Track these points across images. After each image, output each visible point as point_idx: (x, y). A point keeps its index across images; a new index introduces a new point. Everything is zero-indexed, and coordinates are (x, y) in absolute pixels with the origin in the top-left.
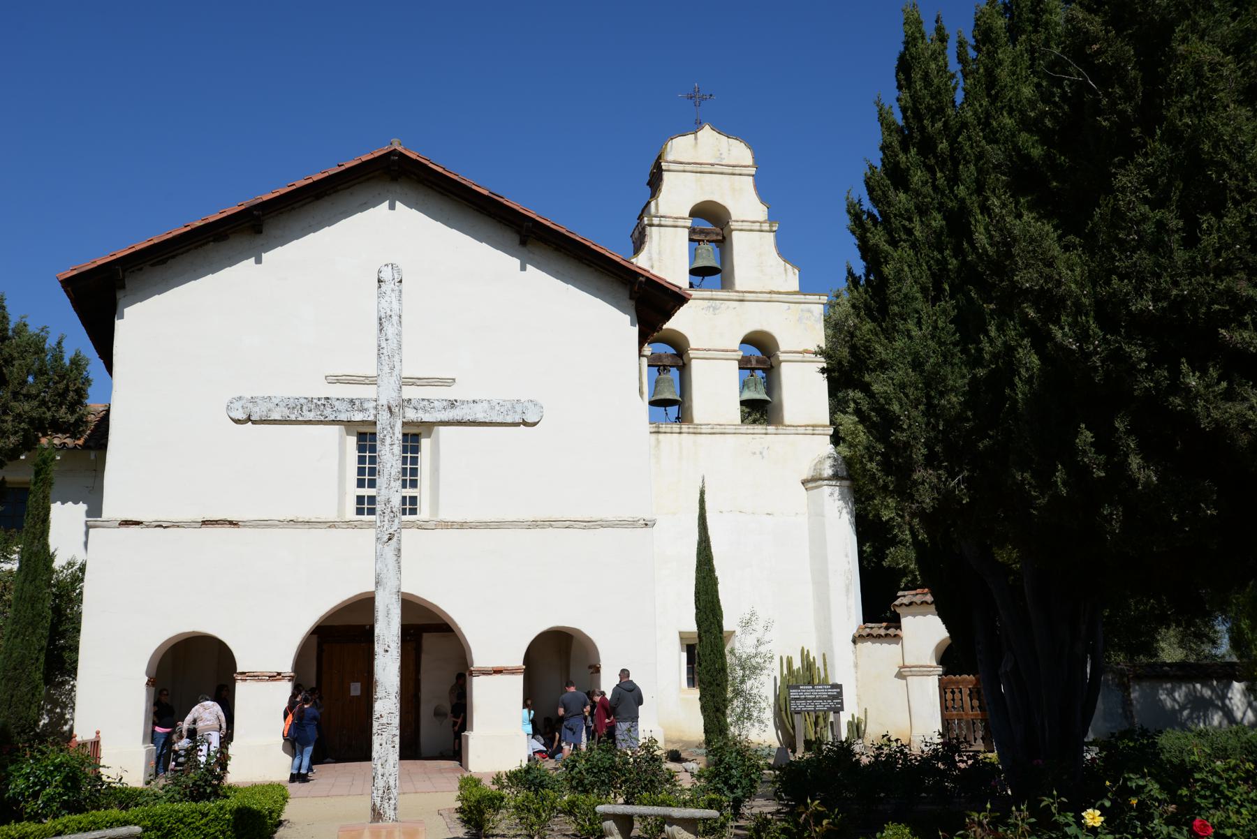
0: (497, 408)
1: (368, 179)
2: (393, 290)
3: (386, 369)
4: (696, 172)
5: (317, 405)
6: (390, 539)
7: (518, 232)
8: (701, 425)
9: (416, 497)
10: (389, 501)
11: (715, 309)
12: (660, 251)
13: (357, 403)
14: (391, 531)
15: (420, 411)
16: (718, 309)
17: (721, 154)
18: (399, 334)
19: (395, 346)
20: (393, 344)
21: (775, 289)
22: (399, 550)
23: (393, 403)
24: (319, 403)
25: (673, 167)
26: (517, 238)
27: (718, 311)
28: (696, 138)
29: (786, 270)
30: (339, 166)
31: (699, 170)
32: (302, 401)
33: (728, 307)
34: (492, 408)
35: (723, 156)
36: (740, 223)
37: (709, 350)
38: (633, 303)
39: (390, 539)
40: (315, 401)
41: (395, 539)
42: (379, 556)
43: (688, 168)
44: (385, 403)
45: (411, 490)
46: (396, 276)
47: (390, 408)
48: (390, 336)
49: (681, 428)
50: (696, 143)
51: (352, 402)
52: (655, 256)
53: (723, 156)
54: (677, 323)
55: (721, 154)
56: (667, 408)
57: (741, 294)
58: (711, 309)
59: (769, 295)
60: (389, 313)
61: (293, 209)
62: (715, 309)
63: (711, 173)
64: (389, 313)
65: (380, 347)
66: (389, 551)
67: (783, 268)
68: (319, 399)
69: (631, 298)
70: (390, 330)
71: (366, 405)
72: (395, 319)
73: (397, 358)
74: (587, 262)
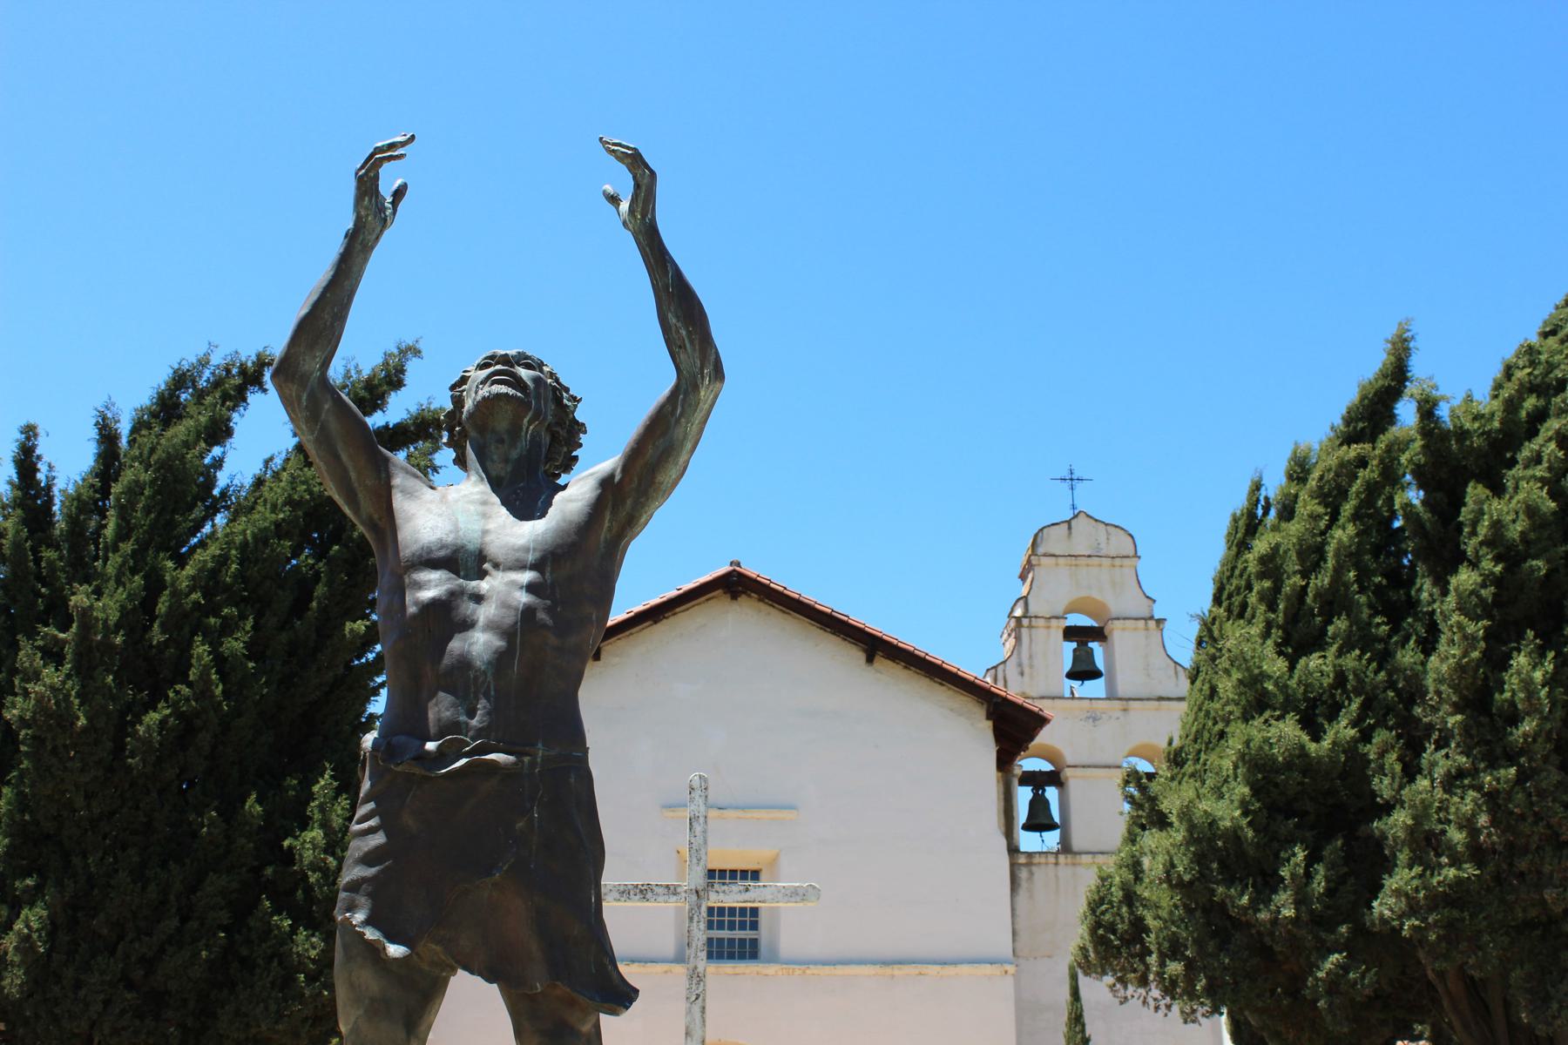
0: (783, 891)
1: (708, 600)
2: (700, 796)
3: (695, 860)
4: (1071, 565)
5: (641, 891)
6: (697, 999)
7: (865, 651)
8: (1080, 853)
9: (756, 939)
10: (696, 968)
11: (1095, 719)
12: (1031, 657)
13: (672, 888)
14: (697, 992)
15: (721, 894)
16: (1100, 719)
17: (1099, 544)
18: (705, 832)
19: (701, 841)
20: (700, 840)
21: (1164, 694)
22: (704, 1008)
23: (700, 888)
24: (643, 888)
25: (1044, 560)
26: (860, 656)
27: (1097, 723)
28: (1070, 528)
29: (1176, 673)
30: (678, 590)
31: (1074, 563)
32: (630, 887)
33: (1110, 717)
34: (779, 892)
35: (1101, 546)
36: (1122, 621)
37: (1089, 766)
38: (990, 723)
39: (697, 999)
40: (640, 887)
41: (700, 999)
42: (689, 1012)
43: (1061, 560)
44: (694, 888)
45: (751, 932)
46: (703, 784)
47: (697, 892)
48: (697, 833)
49: (1057, 858)
50: (1070, 533)
51: (668, 887)
52: (1025, 661)
53: (1101, 546)
54: (1044, 737)
55: (1099, 544)
56: (1043, 834)
57: (1124, 702)
58: (1091, 720)
59: (1156, 703)
60: (697, 814)
61: (631, 634)
62: (1095, 719)
63: (1088, 565)
64: (697, 814)
65: (691, 843)
66: (696, 1008)
67: (1172, 672)
68: (643, 885)
69: (988, 718)
70: (698, 829)
71: (679, 890)
72: (702, 820)
73: (703, 851)
74: (940, 681)
